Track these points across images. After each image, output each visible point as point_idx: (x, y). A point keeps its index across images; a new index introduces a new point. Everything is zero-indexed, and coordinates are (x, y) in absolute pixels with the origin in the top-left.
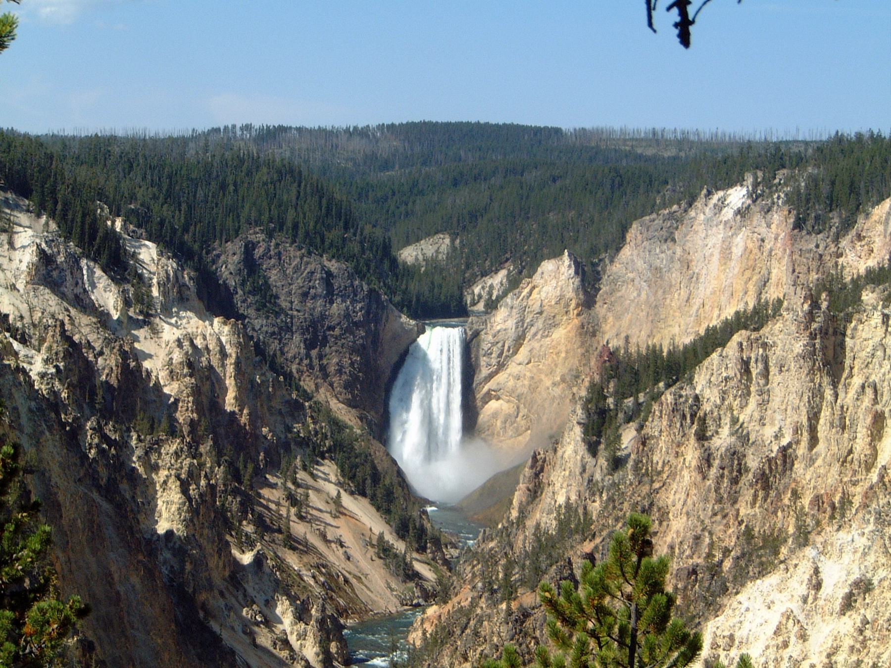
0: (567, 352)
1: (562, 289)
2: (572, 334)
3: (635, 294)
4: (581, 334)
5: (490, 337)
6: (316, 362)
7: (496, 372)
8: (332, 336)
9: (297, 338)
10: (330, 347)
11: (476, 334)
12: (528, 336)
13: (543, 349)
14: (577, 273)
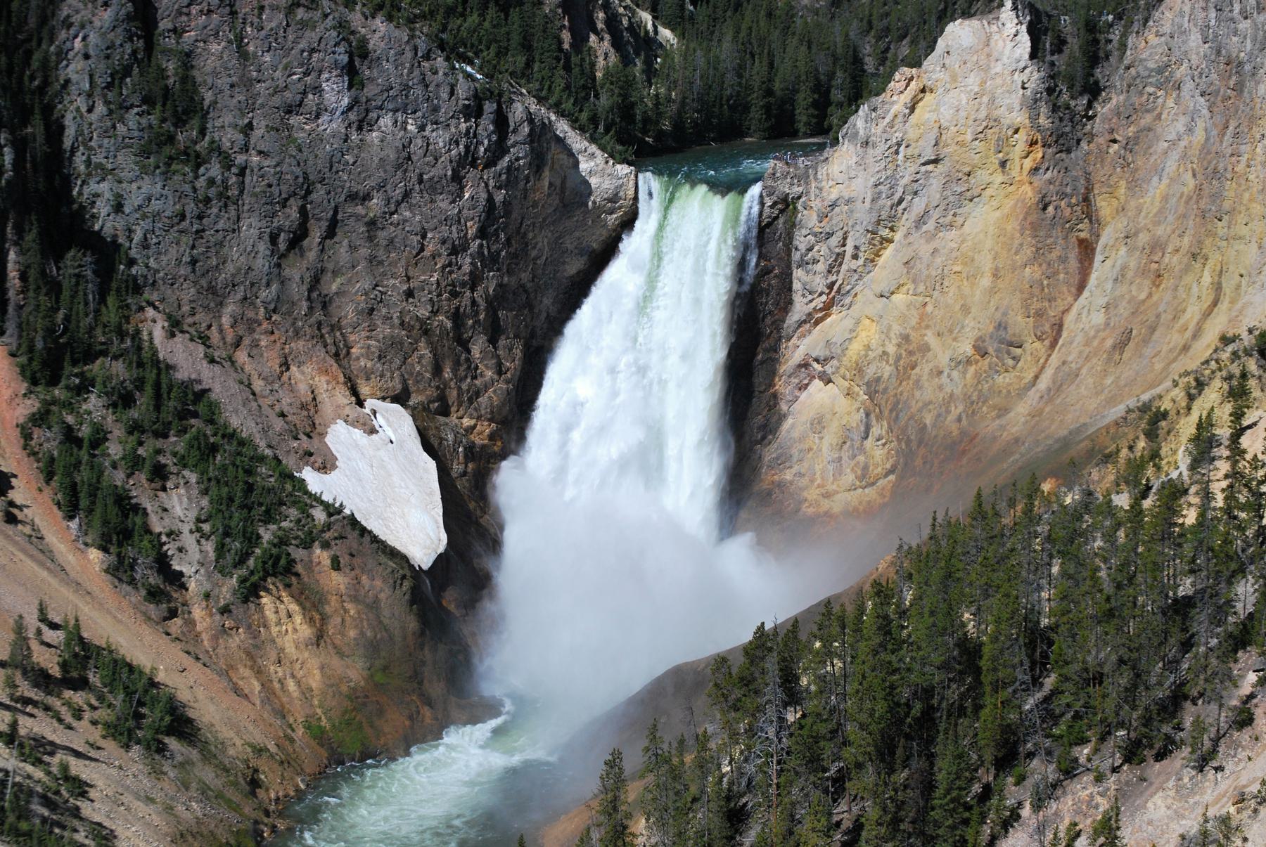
0: (996, 275)
1: (992, 100)
2: (1012, 226)
3: (1180, 126)
4: (1035, 227)
5: (815, 217)
6: (297, 290)
7: (828, 307)
8: (359, 218)
9: (251, 227)
10: (352, 248)
11: (787, 205)
12: (906, 222)
13: (939, 260)
14: (1033, 56)
